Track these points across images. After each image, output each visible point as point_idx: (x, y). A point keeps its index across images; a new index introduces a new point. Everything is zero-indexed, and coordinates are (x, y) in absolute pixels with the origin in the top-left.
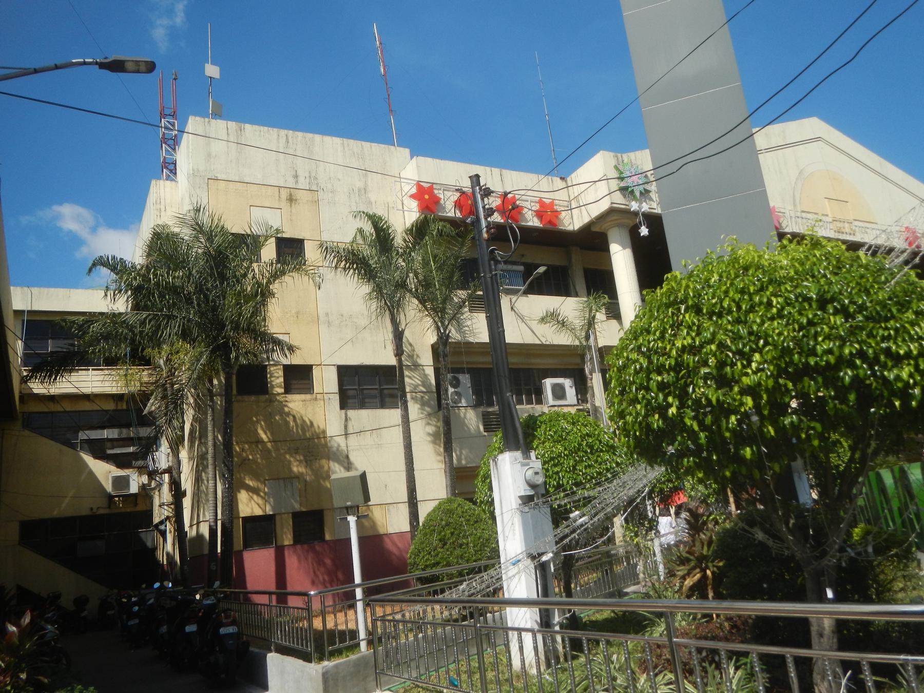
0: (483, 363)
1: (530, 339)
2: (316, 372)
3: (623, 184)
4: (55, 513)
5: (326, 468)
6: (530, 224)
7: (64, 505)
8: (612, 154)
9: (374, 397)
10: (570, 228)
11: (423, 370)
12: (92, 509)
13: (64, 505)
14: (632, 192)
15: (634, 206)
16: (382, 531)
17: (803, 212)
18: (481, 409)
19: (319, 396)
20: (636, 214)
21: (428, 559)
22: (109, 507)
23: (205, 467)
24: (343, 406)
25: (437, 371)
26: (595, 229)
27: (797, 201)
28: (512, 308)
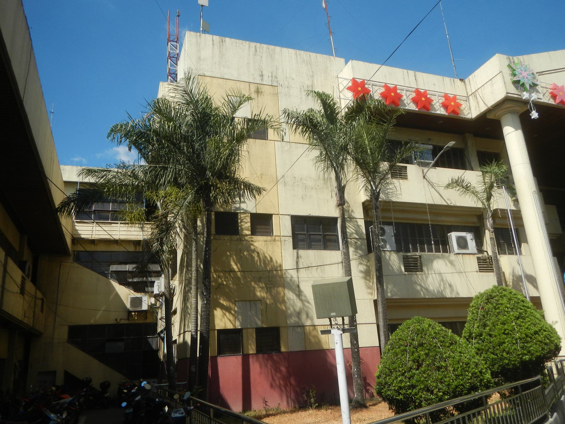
0: (402, 219)
1: (438, 201)
2: (275, 219)
3: (515, 79)
4: (92, 322)
5: (282, 294)
6: (438, 112)
7: (98, 316)
8: (505, 57)
9: (319, 241)
10: (469, 116)
11: (357, 222)
12: (116, 320)
13: (98, 316)
14: (523, 85)
15: (525, 96)
16: (325, 347)
18: (401, 254)
19: (277, 238)
20: (526, 102)
21: (401, 381)
22: (128, 319)
23: (189, 291)
24: (295, 246)
25: (368, 224)
26: (490, 116)
28: (424, 177)
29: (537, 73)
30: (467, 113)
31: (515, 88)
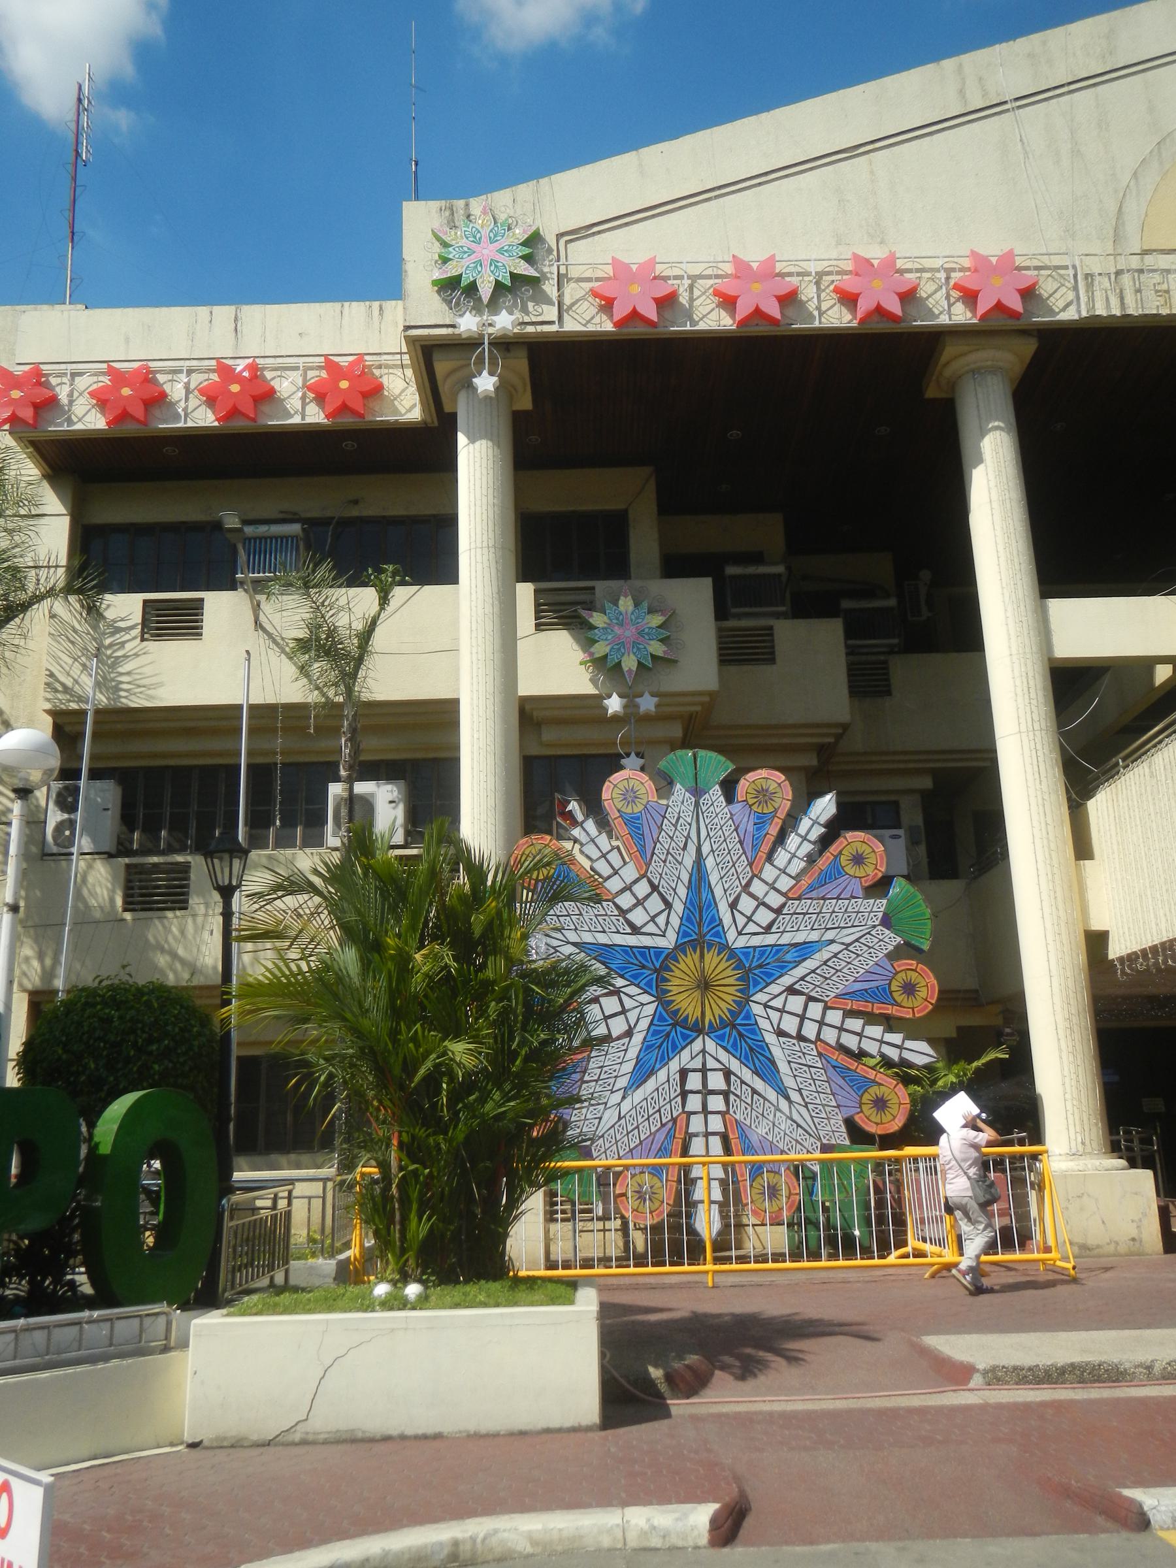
0: (189, 755)
14: (472, 289)
15: (468, 323)
17: (1145, 252)
27: (1131, 227)
29: (560, 236)
30: (408, 405)
31: (445, 307)
